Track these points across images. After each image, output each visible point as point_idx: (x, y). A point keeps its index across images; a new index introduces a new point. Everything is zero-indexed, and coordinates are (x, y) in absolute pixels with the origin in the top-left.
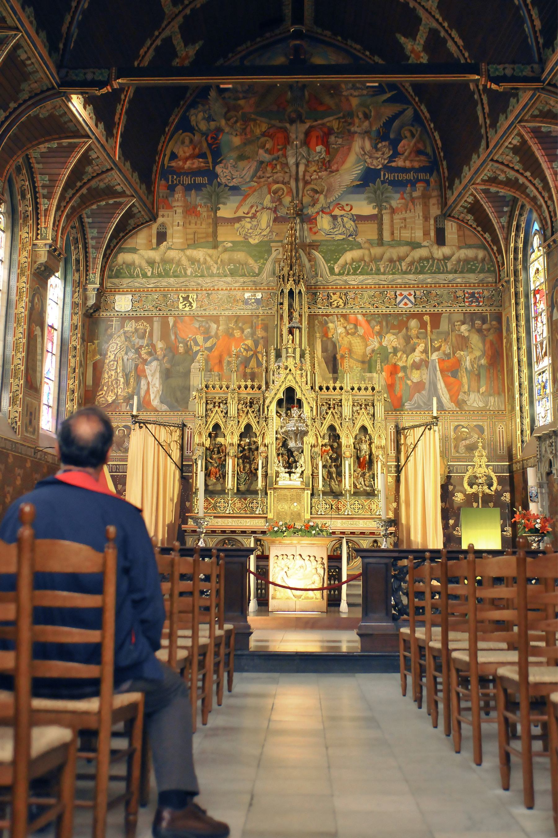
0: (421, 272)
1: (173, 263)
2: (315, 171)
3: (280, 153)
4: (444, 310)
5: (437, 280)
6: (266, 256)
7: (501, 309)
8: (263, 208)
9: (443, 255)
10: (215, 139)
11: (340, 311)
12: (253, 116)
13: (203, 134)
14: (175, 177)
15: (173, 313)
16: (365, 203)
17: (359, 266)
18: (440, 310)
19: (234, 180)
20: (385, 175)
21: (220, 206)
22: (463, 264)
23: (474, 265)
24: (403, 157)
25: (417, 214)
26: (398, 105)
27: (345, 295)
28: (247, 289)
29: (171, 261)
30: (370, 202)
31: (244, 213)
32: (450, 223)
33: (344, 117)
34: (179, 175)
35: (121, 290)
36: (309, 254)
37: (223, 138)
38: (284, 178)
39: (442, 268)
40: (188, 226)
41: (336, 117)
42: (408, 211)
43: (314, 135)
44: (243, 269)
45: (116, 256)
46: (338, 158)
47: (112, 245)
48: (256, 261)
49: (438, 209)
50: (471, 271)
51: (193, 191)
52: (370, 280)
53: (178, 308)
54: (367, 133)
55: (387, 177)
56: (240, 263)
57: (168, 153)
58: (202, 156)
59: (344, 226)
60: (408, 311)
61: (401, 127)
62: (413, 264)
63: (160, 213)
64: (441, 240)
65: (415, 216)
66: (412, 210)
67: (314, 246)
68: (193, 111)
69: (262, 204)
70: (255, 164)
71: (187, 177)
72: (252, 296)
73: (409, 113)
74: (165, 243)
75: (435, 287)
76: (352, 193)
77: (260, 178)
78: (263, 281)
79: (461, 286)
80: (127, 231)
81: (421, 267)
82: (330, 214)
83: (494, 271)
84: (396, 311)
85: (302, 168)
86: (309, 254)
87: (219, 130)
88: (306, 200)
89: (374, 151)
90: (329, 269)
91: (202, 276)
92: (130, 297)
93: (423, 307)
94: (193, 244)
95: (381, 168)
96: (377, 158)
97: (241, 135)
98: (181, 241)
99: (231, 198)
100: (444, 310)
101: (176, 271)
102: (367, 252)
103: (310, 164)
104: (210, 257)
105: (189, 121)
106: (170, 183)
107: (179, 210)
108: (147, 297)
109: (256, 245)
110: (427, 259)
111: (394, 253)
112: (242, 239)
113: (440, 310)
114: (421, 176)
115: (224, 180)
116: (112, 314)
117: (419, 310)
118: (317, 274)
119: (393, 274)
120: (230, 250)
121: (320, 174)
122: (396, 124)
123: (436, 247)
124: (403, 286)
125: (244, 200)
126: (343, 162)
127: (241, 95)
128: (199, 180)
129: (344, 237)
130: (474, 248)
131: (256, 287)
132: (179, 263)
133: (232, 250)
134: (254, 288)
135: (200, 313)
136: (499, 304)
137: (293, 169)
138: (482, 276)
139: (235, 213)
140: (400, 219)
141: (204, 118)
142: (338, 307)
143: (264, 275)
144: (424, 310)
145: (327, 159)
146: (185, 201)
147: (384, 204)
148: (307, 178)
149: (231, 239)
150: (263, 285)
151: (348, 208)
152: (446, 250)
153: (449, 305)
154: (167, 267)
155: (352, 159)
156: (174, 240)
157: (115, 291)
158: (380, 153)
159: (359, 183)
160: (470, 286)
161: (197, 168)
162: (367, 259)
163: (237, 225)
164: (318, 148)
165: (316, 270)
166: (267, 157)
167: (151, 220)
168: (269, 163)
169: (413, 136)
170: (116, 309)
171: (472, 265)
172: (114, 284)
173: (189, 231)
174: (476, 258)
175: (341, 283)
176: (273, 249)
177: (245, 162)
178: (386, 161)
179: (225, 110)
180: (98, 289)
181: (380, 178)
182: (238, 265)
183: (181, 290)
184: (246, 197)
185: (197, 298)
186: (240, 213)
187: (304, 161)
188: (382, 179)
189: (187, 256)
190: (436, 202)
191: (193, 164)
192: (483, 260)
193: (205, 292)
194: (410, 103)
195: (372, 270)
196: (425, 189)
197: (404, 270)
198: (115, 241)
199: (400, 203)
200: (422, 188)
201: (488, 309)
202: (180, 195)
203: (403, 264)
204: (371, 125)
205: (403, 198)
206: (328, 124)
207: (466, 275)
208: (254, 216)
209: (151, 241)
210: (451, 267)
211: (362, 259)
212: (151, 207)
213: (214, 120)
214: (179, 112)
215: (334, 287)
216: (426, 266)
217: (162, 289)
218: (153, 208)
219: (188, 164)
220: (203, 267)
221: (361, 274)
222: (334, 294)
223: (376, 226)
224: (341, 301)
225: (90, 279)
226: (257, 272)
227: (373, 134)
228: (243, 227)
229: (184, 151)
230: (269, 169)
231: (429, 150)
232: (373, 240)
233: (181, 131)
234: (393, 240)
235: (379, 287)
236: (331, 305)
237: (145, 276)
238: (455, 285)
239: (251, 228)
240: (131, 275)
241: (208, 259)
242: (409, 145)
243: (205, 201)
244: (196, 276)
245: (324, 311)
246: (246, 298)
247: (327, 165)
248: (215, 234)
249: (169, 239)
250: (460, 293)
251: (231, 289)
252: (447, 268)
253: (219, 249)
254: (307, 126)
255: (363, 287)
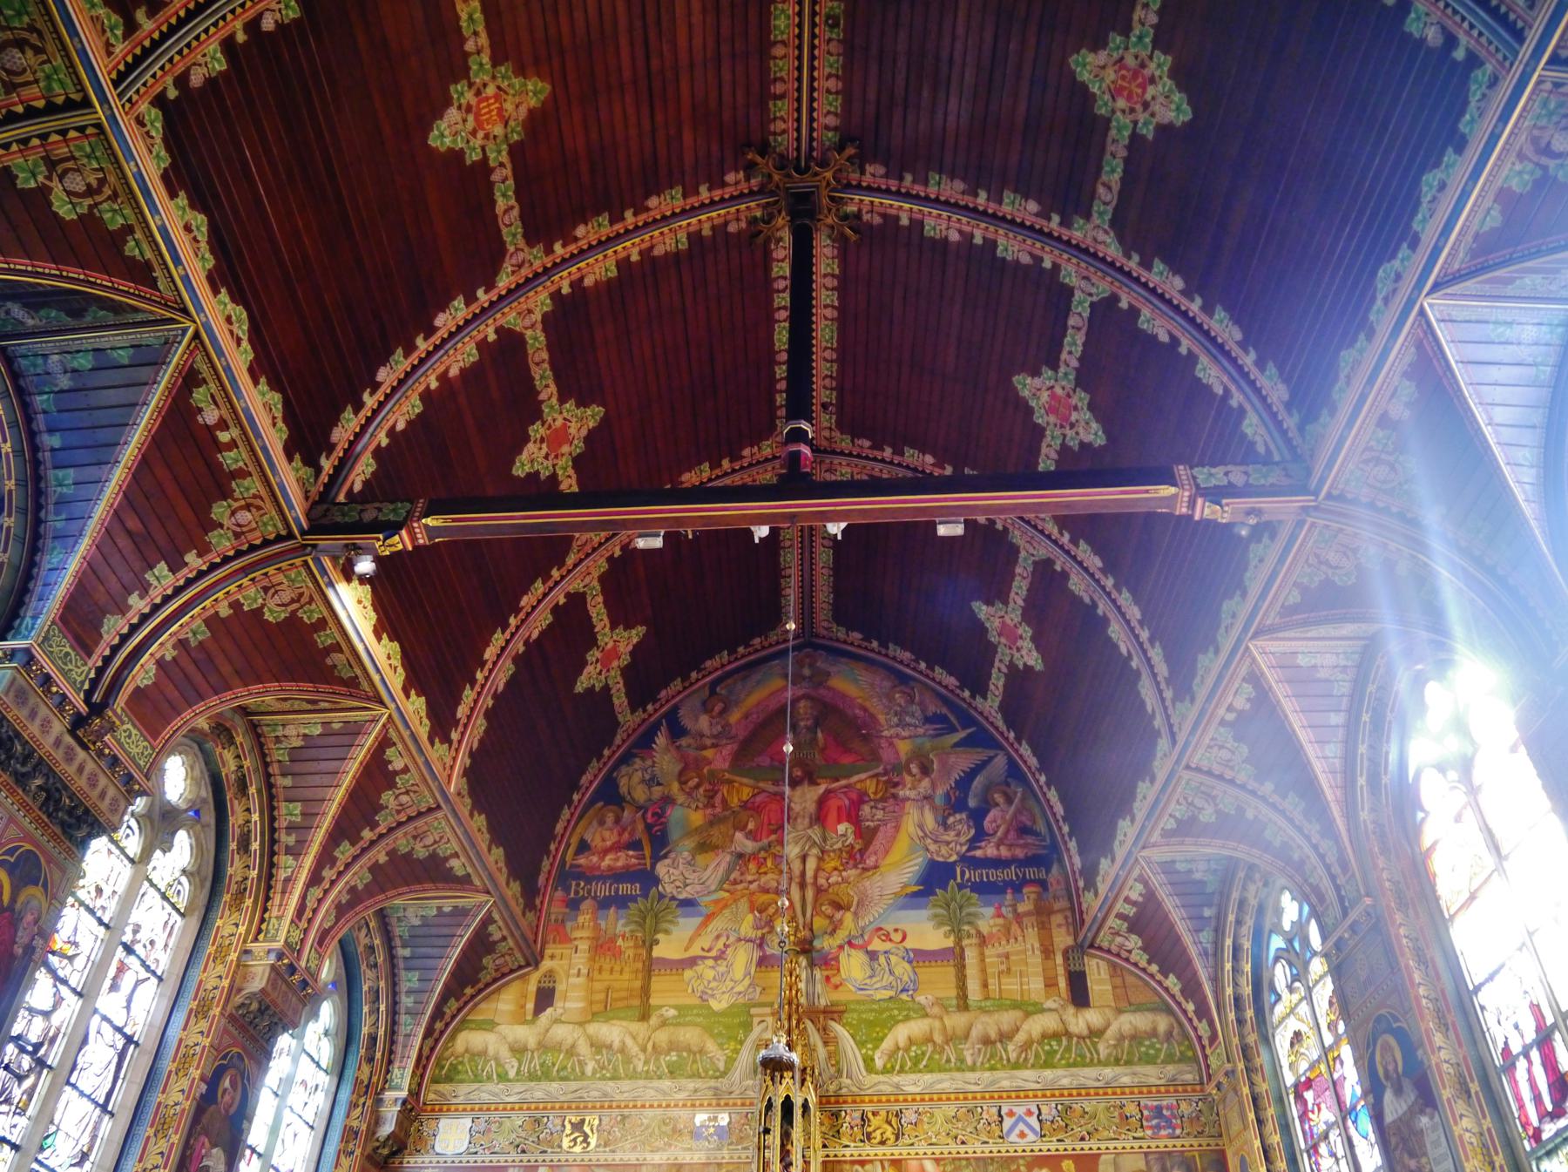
0: (1047, 1065)
1: (560, 1051)
2: (836, 869)
3: (773, 837)
4: (1103, 1147)
5: (1083, 1081)
6: (741, 1036)
7: (1220, 1143)
8: (740, 940)
9: (1089, 1028)
10: (659, 816)
11: (888, 1152)
12: (727, 775)
13: (639, 808)
14: (582, 884)
15: (548, 1159)
16: (930, 925)
17: (924, 1054)
18: (1095, 1147)
19: (688, 888)
20: (963, 874)
21: (660, 936)
22: (1130, 1046)
23: (1152, 1046)
24: (995, 839)
25: (1029, 946)
26: (980, 750)
27: (897, 1115)
28: (701, 1105)
29: (557, 1048)
30: (940, 925)
31: (703, 949)
32: (1094, 962)
33: (886, 773)
34: (588, 881)
35: (453, 1108)
36: (824, 1030)
37: (675, 815)
38: (779, 883)
39: (1088, 1055)
40: (596, 975)
41: (871, 773)
42: (1012, 940)
43: (833, 804)
44: (694, 1061)
45: (453, 1037)
46: (877, 844)
47: (448, 1012)
48: (721, 1046)
49: (1069, 934)
50: (1150, 1060)
51: (612, 910)
52: (945, 1082)
53: (560, 1146)
54: (928, 798)
55: (967, 876)
56: (689, 1051)
57: (574, 841)
58: (635, 845)
59: (891, 973)
60: (1028, 1149)
61: (988, 789)
62: (1030, 1047)
63: (548, 952)
64: (1079, 995)
65: (1025, 951)
66: (1020, 938)
67: (833, 1013)
68: (624, 769)
69: (737, 931)
70: (728, 858)
71: (604, 883)
72: (710, 1119)
73: (1000, 762)
74: (549, 1010)
75: (1079, 1095)
76: (904, 907)
77: (735, 882)
78: (734, 1088)
79: (1132, 1093)
80: (481, 985)
81: (1048, 1053)
82: (863, 947)
83: (1195, 1059)
84: (1003, 1150)
85: (811, 864)
86: (824, 1029)
87: (668, 800)
88: (819, 923)
89: (941, 829)
90: (865, 1061)
91: (613, 1078)
92: (467, 1122)
93: (1059, 1140)
94: (602, 1010)
95: (955, 862)
96: (948, 843)
97: (706, 807)
98: (581, 1005)
99: (681, 920)
100: (1103, 1147)
101: (565, 1068)
102: (937, 1024)
103: (826, 857)
104: (634, 1038)
105: (617, 786)
106: (572, 895)
107: (583, 946)
108: (501, 1124)
109: (723, 1014)
110: (1056, 1036)
111: (988, 1024)
112: (698, 1002)
113: (1095, 1147)
114: (1031, 873)
115: (669, 889)
116: (427, 1160)
117: (1051, 1146)
118: (839, 1072)
119: (992, 1068)
120: (672, 1024)
121: (844, 874)
122: (978, 782)
123: (1071, 1010)
124: (1013, 1094)
125: (704, 924)
126: (887, 852)
127: (708, 742)
128: (625, 889)
129: (892, 993)
130: (1148, 1010)
131: (719, 1100)
132: (571, 1051)
133: (677, 1023)
134: (714, 1102)
135: (602, 1158)
136: (1214, 1131)
137: (797, 867)
138: (1171, 1069)
139: (686, 950)
140: (999, 956)
141: (643, 781)
142: (883, 1143)
143: (736, 1075)
144: (1061, 1148)
145: (857, 847)
146: (597, 927)
147: (966, 928)
148: (821, 881)
149: (673, 1001)
150: (733, 1096)
151: (897, 937)
152: (1092, 1017)
153: (1112, 1135)
154: (549, 1058)
155: (902, 844)
156: (568, 1005)
157: (441, 1110)
158: (953, 833)
159: (916, 889)
160: (1150, 1092)
161: (623, 867)
162: (938, 1038)
163: (688, 974)
164: (841, 828)
165: (838, 1063)
166: (749, 846)
167: (528, 965)
168: (754, 856)
169: (1009, 801)
170: (438, 1149)
171: (1149, 1047)
172: (442, 1095)
173: (598, 986)
174: (1154, 1033)
175: (889, 1089)
176: (756, 1020)
177: (711, 854)
178: (965, 848)
179: (682, 765)
180: (405, 1102)
181: (955, 879)
182: (685, 1054)
183: (569, 1108)
184: (709, 918)
185: (600, 1125)
186: (695, 951)
187: (815, 851)
188: (959, 880)
189: (589, 1037)
190: (1064, 922)
191: (617, 859)
192: (1169, 1035)
193: (616, 1112)
194: (1000, 747)
195: (948, 1061)
196: (1039, 898)
197: (1012, 1060)
198: (453, 1005)
199: (996, 925)
200: (1033, 896)
201: (1196, 1144)
202: (588, 917)
203: (1010, 1047)
204: (934, 786)
205: (999, 915)
206: (858, 786)
207: (1138, 1069)
208: (720, 957)
209: (523, 1007)
210: (1107, 1051)
211: (929, 1039)
212: (531, 937)
213: (659, 784)
214: (600, 770)
215: (875, 1098)
216: (1056, 1052)
217: (533, 1106)
218: (535, 941)
219: (608, 861)
220: (617, 1060)
221: (929, 1069)
222: (874, 1114)
223: (950, 972)
224: (890, 1129)
225: (392, 1080)
226: (722, 1069)
227: (939, 800)
228: (700, 977)
229: (601, 835)
230: (752, 866)
231: (1041, 827)
232: (948, 999)
233: (600, 804)
234: (987, 998)
235: (965, 1099)
236: (869, 1138)
237: (503, 1077)
238: (1118, 1090)
239: (714, 979)
240: (476, 1076)
241: (629, 1042)
242: (1003, 818)
243: (632, 927)
244: (603, 1078)
245: (856, 1153)
246: (698, 1124)
247: (858, 856)
248: (645, 992)
249: (558, 1003)
250: (1131, 1109)
251: (668, 1106)
252: (1098, 1054)
253: (651, 1022)
254: (821, 789)
255: (934, 1098)
